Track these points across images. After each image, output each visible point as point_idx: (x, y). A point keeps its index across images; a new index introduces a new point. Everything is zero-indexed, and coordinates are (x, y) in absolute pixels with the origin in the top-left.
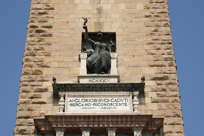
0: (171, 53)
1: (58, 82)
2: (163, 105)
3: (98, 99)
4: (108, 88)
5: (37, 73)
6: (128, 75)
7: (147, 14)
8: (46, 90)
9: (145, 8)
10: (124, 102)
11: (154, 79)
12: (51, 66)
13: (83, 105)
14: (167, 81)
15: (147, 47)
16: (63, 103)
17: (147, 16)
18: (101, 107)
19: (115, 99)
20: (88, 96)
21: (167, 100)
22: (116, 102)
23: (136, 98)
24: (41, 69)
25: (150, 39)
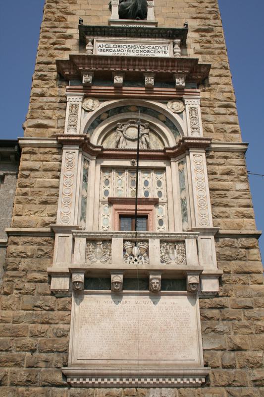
1: (84, 24)
3: (133, 45)
4: (145, 33)
5: (59, 20)
8: (71, 37)
10: (163, 49)
11: (197, 31)
12: (77, 14)
13: (114, 51)
14: (212, 34)
16: (92, 48)
19: (152, 46)
20: (121, 42)
21: (212, 52)
22: (153, 49)
23: (177, 46)
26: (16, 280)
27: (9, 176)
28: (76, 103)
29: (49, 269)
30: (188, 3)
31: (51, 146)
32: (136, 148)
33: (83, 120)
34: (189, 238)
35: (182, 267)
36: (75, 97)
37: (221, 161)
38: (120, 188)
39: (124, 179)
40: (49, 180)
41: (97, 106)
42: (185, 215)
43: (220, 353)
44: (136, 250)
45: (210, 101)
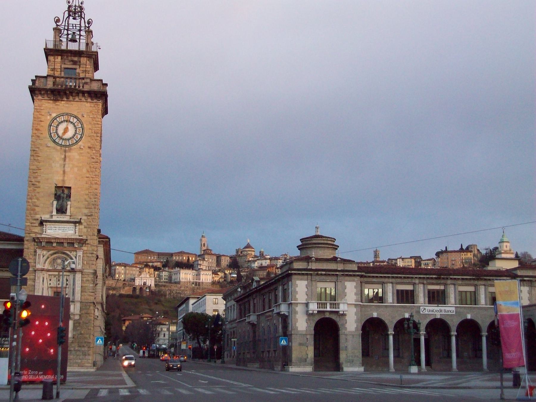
1: (43, 219)
7: (88, 175)
11: (86, 216)
14: (92, 217)
17: (87, 177)
33: (42, 260)
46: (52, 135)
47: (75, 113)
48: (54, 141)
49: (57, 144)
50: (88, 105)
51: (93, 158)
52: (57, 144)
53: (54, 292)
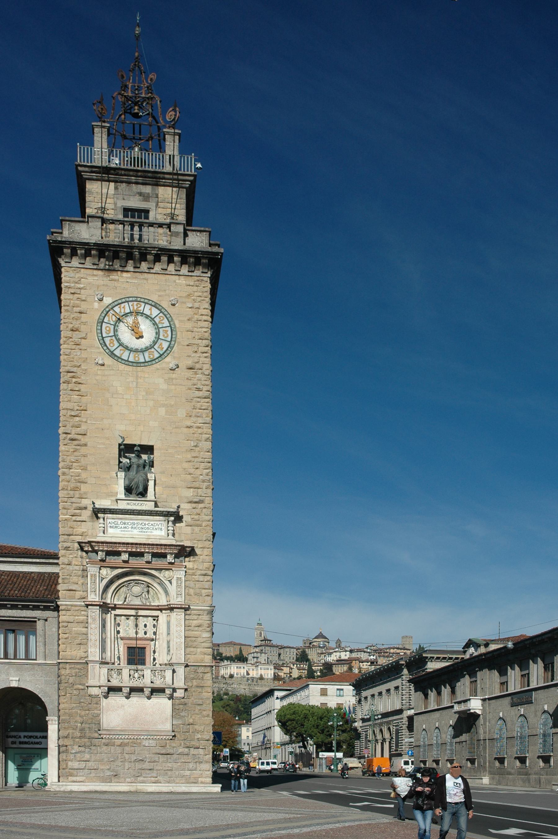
0: (209, 474)
2: (197, 529)
3: (136, 522)
5: (75, 489)
6: (164, 496)
7: (189, 423)
8: (85, 508)
9: (186, 416)
10: (160, 526)
11: (190, 502)
12: (89, 482)
13: (121, 528)
15: (186, 465)
16: (103, 526)
18: (138, 530)
19: (151, 523)
22: (152, 526)
23: (170, 523)
24: (79, 484)
25: (189, 456)
26: (68, 688)
27: (50, 619)
28: (95, 573)
29: (87, 685)
30: (185, 469)
31: (80, 606)
32: (160, 338)
34: (168, 669)
35: (162, 686)
36: (93, 569)
37: (195, 617)
38: (127, 629)
39: (130, 623)
40: (80, 629)
41: (107, 573)
42: (169, 651)
43: (181, 725)
44: (136, 675)
45: (193, 570)
46: (107, 341)
47: (155, 298)
48: (112, 354)
49: (118, 359)
50: (182, 281)
51: (199, 389)
52: (118, 359)
53: (128, 647)
